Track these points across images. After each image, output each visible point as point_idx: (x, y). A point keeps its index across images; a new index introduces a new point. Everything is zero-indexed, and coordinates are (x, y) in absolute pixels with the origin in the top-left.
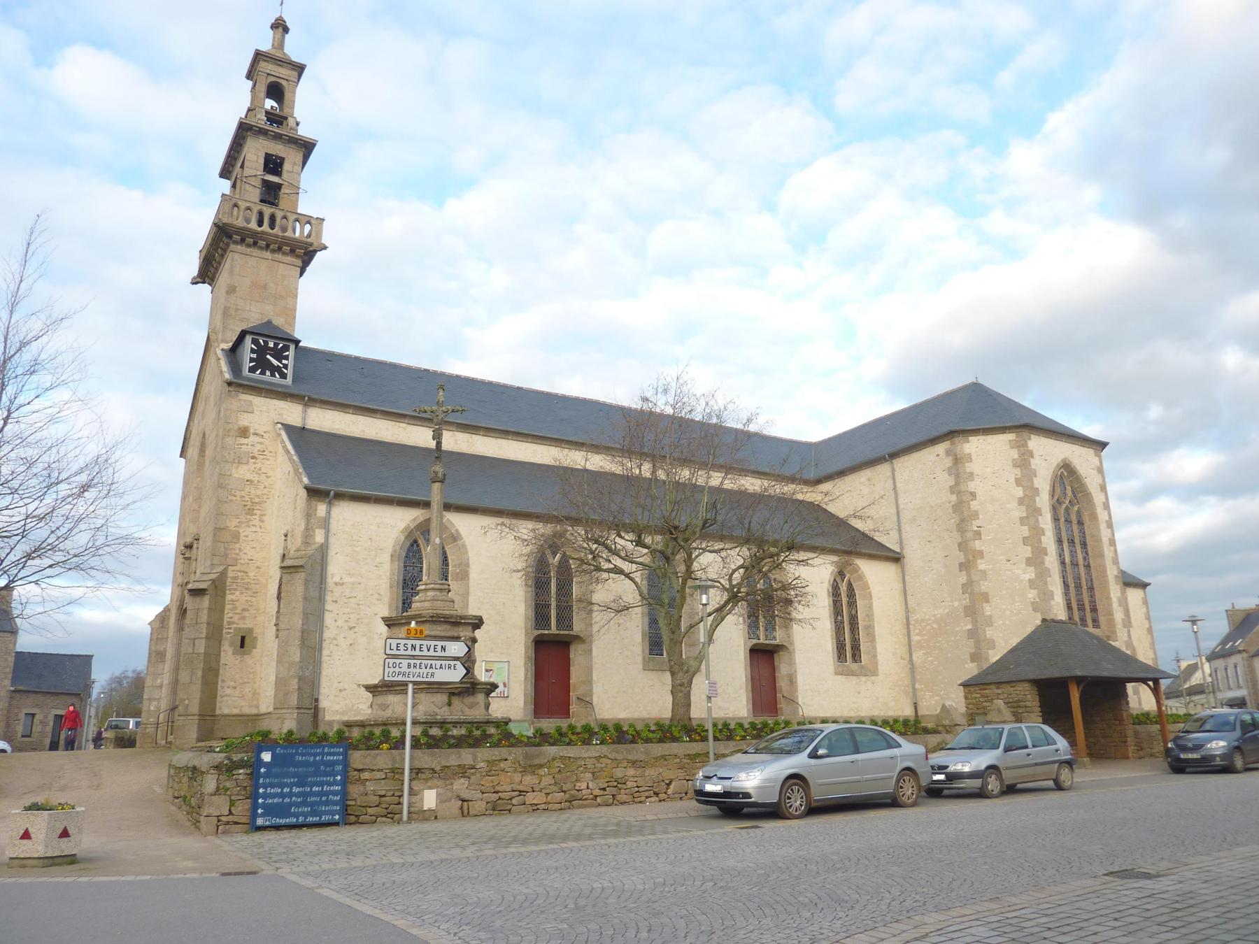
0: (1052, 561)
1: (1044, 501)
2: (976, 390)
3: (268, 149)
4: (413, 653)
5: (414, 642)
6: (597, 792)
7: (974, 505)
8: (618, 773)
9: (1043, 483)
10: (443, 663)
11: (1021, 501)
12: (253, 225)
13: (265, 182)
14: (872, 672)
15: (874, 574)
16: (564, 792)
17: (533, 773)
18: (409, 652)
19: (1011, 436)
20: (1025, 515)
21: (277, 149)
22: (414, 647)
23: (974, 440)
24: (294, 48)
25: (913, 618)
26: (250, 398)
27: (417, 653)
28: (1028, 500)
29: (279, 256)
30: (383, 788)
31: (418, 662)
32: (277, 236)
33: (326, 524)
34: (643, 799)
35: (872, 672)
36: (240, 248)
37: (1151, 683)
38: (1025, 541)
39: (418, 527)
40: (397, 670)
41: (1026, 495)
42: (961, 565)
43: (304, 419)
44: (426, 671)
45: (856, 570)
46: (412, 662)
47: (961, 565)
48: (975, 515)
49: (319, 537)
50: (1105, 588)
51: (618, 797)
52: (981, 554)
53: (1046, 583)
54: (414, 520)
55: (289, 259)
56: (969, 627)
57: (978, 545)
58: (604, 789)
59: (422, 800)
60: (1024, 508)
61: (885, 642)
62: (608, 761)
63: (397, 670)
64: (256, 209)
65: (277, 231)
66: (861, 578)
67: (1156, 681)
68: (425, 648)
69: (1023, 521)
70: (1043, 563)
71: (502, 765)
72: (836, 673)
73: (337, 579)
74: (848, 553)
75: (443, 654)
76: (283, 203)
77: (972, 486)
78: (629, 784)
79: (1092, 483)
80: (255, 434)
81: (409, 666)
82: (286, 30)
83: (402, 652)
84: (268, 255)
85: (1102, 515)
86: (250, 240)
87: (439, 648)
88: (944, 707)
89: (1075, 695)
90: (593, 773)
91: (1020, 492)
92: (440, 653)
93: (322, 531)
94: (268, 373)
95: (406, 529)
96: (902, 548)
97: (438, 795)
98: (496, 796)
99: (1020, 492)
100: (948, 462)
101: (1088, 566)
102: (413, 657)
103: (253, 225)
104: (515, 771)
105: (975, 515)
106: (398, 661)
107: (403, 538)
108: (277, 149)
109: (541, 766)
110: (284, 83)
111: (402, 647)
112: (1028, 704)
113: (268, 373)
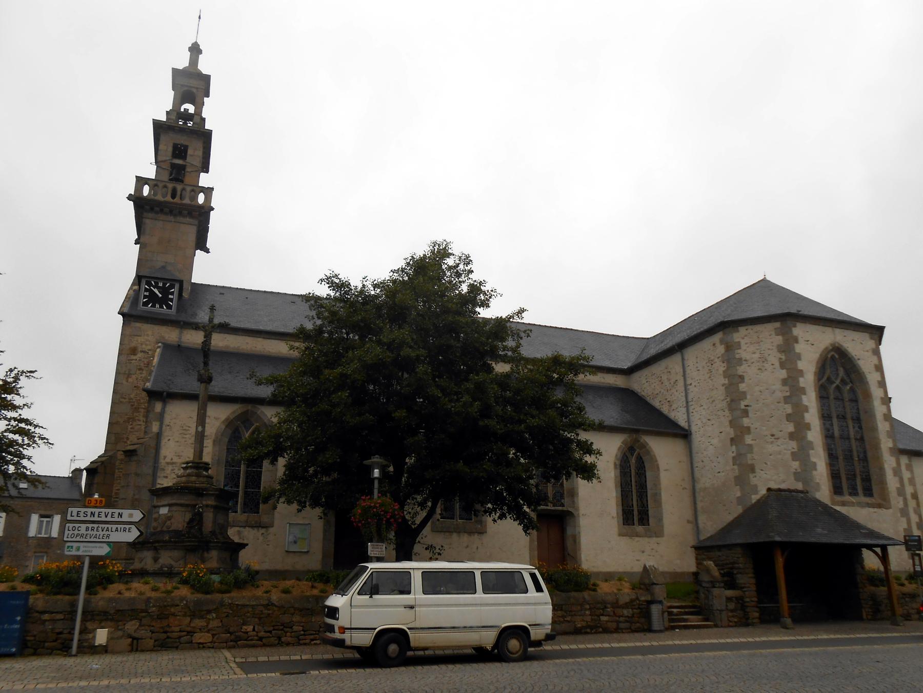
0: (815, 435)
1: (808, 380)
2: (764, 287)
3: (183, 142)
4: (92, 519)
5: (93, 510)
6: (262, 634)
7: (742, 387)
8: (286, 619)
9: (808, 365)
10: (119, 526)
11: (785, 382)
12: (169, 198)
13: (173, 166)
14: (659, 533)
15: (663, 450)
16: (231, 633)
17: (201, 617)
18: (88, 518)
19: (778, 325)
20: (788, 394)
21: (182, 140)
22: (93, 514)
23: (743, 330)
24: (204, 66)
25: (699, 486)
26: (138, 325)
27: (96, 518)
28: (792, 381)
29: (181, 219)
30: (59, 627)
31: (96, 526)
32: (176, 204)
33: (161, 417)
34: (307, 641)
35: (659, 533)
36: (150, 215)
37: (878, 550)
38: (789, 417)
39: (238, 418)
40: (76, 532)
41: (789, 377)
42: (732, 439)
43: (180, 338)
44: (102, 533)
45: (644, 446)
46: (90, 526)
47: (732, 439)
48: (743, 395)
49: (155, 428)
50: (879, 458)
51: (283, 639)
52: (748, 430)
53: (808, 455)
54: (234, 412)
55: (188, 220)
56: (739, 494)
57: (746, 422)
58: (270, 632)
59: (94, 637)
60: (787, 388)
61: (672, 507)
62: (275, 608)
63: (76, 532)
64: (170, 186)
65: (177, 200)
66: (648, 452)
67: (884, 548)
68: (103, 515)
69: (787, 400)
70: (805, 437)
71: (172, 610)
72: (620, 535)
73: (168, 460)
74: (637, 431)
75: (120, 519)
76: (187, 180)
77: (741, 370)
78: (295, 628)
79: (866, 365)
80: (142, 352)
81: (87, 529)
82: (200, 52)
83: (82, 518)
84: (171, 218)
85: (877, 393)
86: (157, 209)
87: (116, 515)
88: (645, 567)
89: (780, 562)
90: (260, 619)
91: (783, 374)
92: (116, 519)
93: (158, 423)
94: (157, 306)
95: (226, 419)
96: (689, 426)
97: (109, 633)
98: (163, 636)
99: (783, 374)
100: (721, 349)
101: (862, 439)
102: (93, 522)
103: (169, 198)
104: (185, 615)
105: (743, 395)
106: (77, 525)
107: (223, 427)
108: (182, 140)
109: (209, 612)
110: (194, 91)
111: (82, 514)
112: (741, 566)
113: (157, 306)
